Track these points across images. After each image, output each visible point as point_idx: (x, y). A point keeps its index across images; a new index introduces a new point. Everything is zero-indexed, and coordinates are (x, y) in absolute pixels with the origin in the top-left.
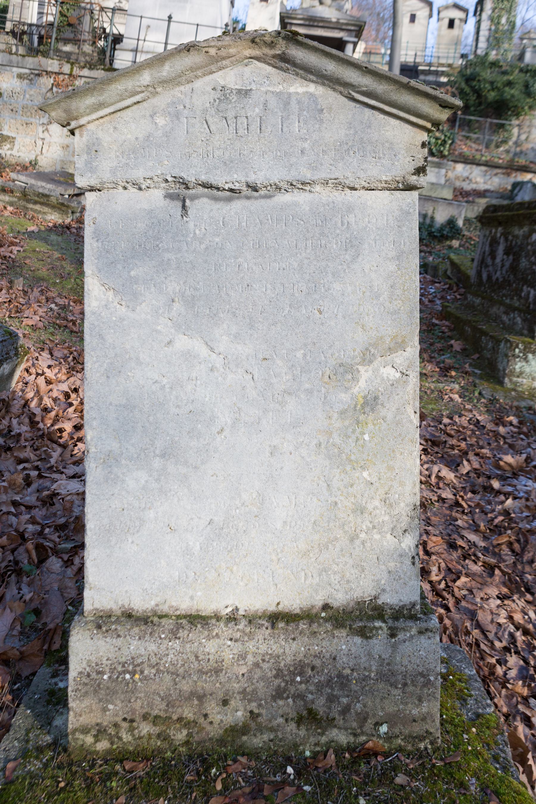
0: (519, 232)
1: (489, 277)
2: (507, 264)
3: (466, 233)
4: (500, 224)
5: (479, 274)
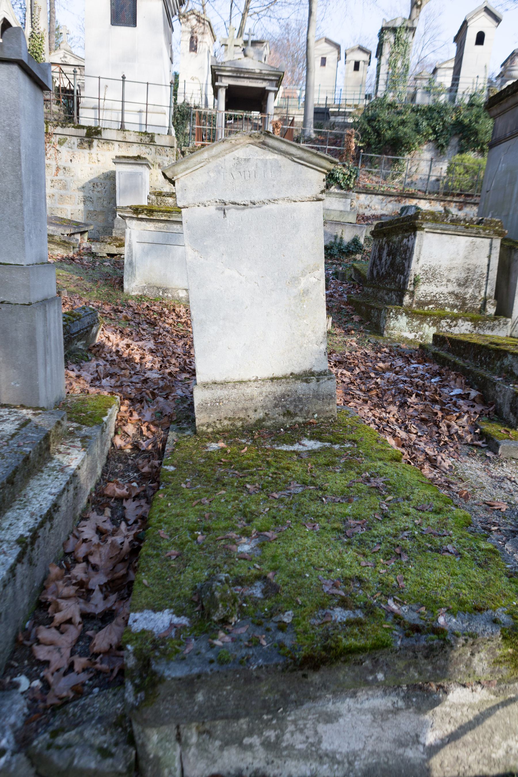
0: (396, 239)
1: (378, 273)
2: (389, 262)
3: (366, 249)
4: (385, 235)
5: (372, 272)
